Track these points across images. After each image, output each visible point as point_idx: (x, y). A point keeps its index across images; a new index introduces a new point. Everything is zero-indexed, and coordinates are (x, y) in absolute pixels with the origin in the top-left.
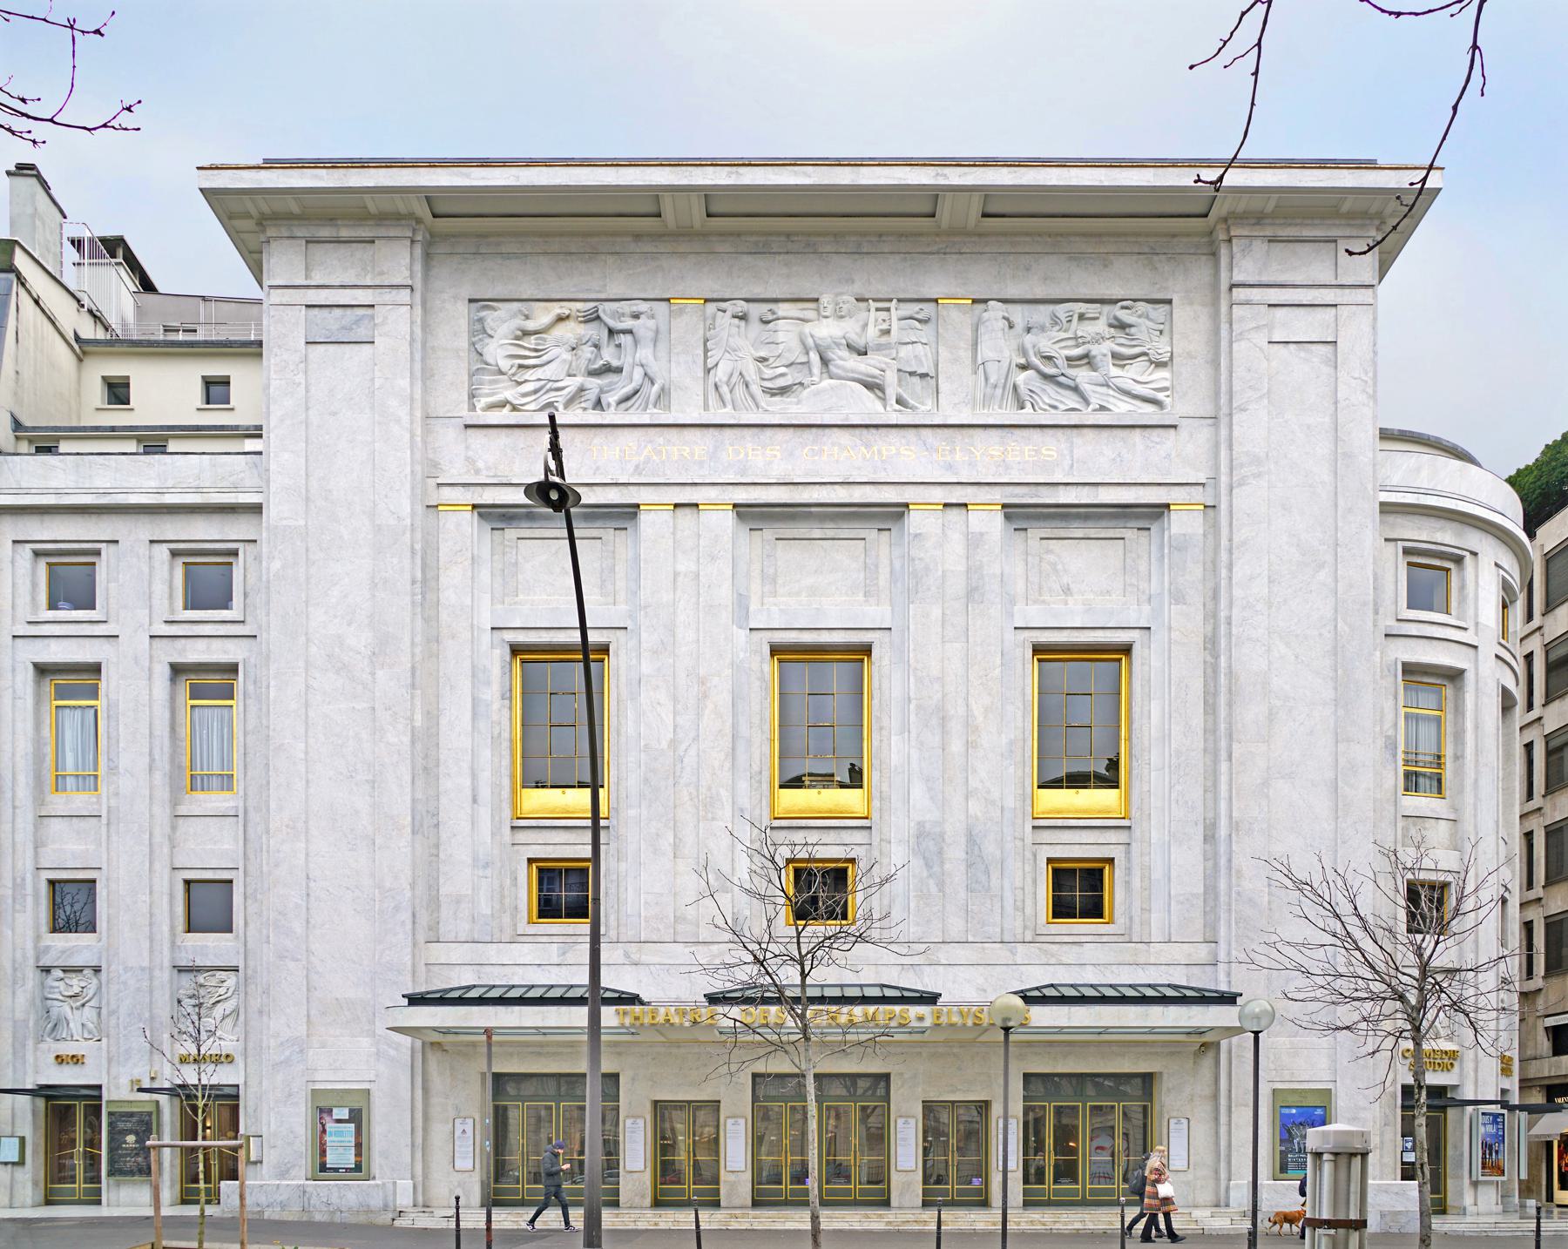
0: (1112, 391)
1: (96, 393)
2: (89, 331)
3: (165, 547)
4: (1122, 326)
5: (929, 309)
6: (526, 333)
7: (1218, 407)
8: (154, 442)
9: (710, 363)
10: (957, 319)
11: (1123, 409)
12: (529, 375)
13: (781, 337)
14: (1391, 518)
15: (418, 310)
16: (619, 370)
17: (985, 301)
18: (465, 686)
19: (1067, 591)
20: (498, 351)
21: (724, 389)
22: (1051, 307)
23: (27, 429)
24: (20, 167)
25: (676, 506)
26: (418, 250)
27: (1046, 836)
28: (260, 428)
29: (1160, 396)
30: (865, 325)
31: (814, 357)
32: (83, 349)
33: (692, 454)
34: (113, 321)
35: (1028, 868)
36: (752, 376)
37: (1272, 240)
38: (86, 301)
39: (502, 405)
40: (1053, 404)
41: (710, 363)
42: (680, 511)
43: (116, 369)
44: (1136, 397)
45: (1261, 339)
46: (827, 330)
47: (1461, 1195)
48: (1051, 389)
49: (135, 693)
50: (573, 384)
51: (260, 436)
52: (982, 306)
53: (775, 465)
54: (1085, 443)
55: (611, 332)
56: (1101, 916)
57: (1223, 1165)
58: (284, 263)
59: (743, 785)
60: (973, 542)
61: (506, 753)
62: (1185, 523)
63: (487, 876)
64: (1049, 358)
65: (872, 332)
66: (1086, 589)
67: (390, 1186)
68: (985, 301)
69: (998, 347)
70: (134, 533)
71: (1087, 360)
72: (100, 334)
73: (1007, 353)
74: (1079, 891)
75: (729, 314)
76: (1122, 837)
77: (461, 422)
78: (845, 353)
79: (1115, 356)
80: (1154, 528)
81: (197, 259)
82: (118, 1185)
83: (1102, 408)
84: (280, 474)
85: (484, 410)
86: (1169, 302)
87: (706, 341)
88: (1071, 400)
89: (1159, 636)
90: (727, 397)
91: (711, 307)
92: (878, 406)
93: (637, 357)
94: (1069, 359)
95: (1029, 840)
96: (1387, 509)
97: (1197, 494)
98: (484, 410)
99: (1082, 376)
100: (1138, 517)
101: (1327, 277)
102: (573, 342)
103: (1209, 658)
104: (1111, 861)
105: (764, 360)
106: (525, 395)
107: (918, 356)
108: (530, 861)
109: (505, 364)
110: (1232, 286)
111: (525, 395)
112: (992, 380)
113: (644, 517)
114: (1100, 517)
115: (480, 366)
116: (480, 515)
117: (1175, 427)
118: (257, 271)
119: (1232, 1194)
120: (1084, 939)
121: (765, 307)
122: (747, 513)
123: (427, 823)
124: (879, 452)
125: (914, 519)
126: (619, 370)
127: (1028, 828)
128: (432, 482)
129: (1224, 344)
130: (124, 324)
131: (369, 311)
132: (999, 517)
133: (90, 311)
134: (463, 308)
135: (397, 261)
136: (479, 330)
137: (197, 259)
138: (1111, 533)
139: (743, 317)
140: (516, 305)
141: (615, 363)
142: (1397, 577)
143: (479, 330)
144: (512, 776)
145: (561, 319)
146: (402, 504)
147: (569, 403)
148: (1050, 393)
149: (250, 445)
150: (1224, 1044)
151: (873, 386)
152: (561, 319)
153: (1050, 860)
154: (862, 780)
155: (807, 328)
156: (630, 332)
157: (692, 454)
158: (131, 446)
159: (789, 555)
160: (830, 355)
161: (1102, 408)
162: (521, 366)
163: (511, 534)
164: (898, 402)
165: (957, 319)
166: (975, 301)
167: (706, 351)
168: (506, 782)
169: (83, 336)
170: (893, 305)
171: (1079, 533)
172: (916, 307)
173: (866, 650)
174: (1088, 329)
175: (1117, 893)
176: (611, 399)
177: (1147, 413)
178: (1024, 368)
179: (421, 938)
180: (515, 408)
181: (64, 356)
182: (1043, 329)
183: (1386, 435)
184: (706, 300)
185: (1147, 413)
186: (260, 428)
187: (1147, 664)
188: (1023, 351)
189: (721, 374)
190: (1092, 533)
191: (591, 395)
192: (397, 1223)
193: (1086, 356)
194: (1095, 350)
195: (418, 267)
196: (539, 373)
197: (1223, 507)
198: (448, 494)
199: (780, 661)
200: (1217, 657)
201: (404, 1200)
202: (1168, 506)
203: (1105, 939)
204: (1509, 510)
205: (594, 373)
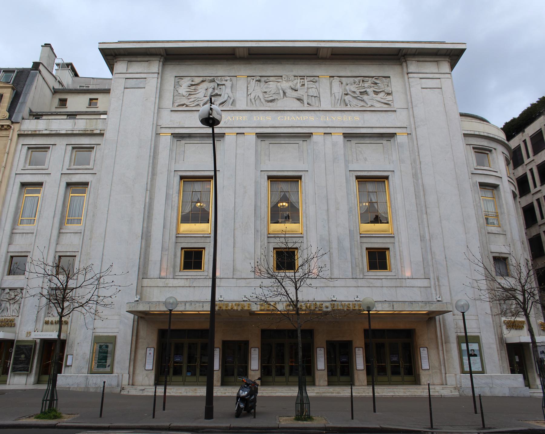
1: (56, 102)
2: (57, 86)
3: (71, 146)
4: (376, 84)
5: (317, 78)
7: (408, 106)
8: (72, 115)
9: (249, 93)
10: (324, 83)
11: (379, 106)
12: (192, 96)
13: (271, 86)
14: (467, 138)
15: (160, 79)
16: (220, 95)
17: (333, 77)
18: (164, 189)
19: (366, 159)
20: (183, 90)
21: (253, 100)
22: (353, 78)
23: (33, 112)
24: (46, 44)
25: (237, 134)
26: (161, 63)
27: (365, 240)
28: (107, 112)
29: (390, 102)
32: (55, 92)
33: (243, 118)
34: (65, 84)
35: (359, 251)
36: (261, 96)
37: (418, 61)
38: (58, 79)
39: (183, 105)
40: (355, 104)
41: (249, 93)
42: (238, 135)
43: (63, 96)
44: (382, 103)
45: (419, 87)
46: (285, 85)
47: (535, 380)
48: (355, 100)
49: (53, 192)
51: (106, 114)
52: (332, 78)
53: (268, 121)
54: (367, 115)
55: (218, 85)
56: (386, 269)
57: (442, 367)
58: (120, 66)
59: (258, 222)
60: (334, 145)
61: (176, 211)
62: (401, 138)
63: (164, 255)
64: (354, 92)
65: (299, 85)
67: (121, 376)
68: (333, 77)
69: (337, 89)
70: (61, 143)
71: (365, 93)
72: (61, 87)
73: (341, 90)
74: (378, 259)
75: (255, 80)
76: (391, 240)
77: (170, 110)
78: (291, 91)
79: (374, 91)
80: (392, 140)
81: (94, 68)
82: (15, 375)
83: (372, 106)
84: (110, 125)
85: (177, 106)
86: (389, 77)
87: (247, 87)
88: (362, 104)
89: (397, 173)
90: (254, 103)
91: (249, 78)
92: (302, 105)
93: (226, 92)
94: (360, 92)
95: (359, 242)
96: (465, 135)
97: (404, 130)
98: (177, 106)
99: (365, 97)
100: (386, 137)
101: (436, 71)
102: (206, 88)
103: (415, 181)
104: (388, 249)
105: (266, 92)
106: (191, 102)
107: (313, 92)
108: (182, 249)
109: (185, 94)
110: (408, 74)
111: (191, 102)
112: (337, 98)
113: (226, 137)
115: (176, 94)
116: (173, 136)
117: (395, 111)
118: (111, 69)
119: (448, 379)
120: (381, 277)
121: (266, 78)
122: (260, 136)
123: (146, 236)
124: (303, 118)
125: (314, 138)
126: (220, 95)
127: (359, 237)
128: (159, 127)
129: (408, 89)
130: (68, 85)
131: (145, 80)
132: (342, 137)
133: (59, 81)
134: (173, 79)
135: (155, 66)
136: (177, 85)
137: (94, 68)
138: (378, 142)
139: (259, 81)
140: (189, 78)
141: (219, 93)
142: (472, 156)
143: (177, 85)
144: (178, 219)
145: (203, 81)
146: (149, 133)
148: (355, 102)
149: (103, 117)
150: (437, 317)
152: (203, 81)
153: (367, 249)
154: (299, 220)
155: (279, 84)
156: (224, 85)
157: (243, 118)
158: (65, 117)
159: (274, 149)
160: (286, 91)
163: (183, 142)
164: (308, 104)
165: (324, 83)
166: (330, 77)
167: (247, 90)
168: (175, 221)
169: (55, 88)
170: (305, 78)
171: (368, 142)
172: (313, 78)
173: (300, 177)
174: (366, 85)
175: (392, 259)
177: (386, 108)
178: (347, 94)
179: (141, 277)
180: (187, 106)
181: (49, 93)
182: (351, 85)
183: (462, 115)
184: (248, 76)
185: (386, 108)
186: (107, 112)
187: (394, 181)
188: (346, 90)
189: (252, 96)
190: (372, 142)
192: (122, 393)
193: (366, 91)
194: (368, 90)
195: (161, 68)
196: (195, 96)
197: (414, 134)
198: (163, 130)
199: (271, 181)
200: (417, 180)
201: (125, 382)
202: (396, 134)
203: (389, 277)
204: (502, 136)
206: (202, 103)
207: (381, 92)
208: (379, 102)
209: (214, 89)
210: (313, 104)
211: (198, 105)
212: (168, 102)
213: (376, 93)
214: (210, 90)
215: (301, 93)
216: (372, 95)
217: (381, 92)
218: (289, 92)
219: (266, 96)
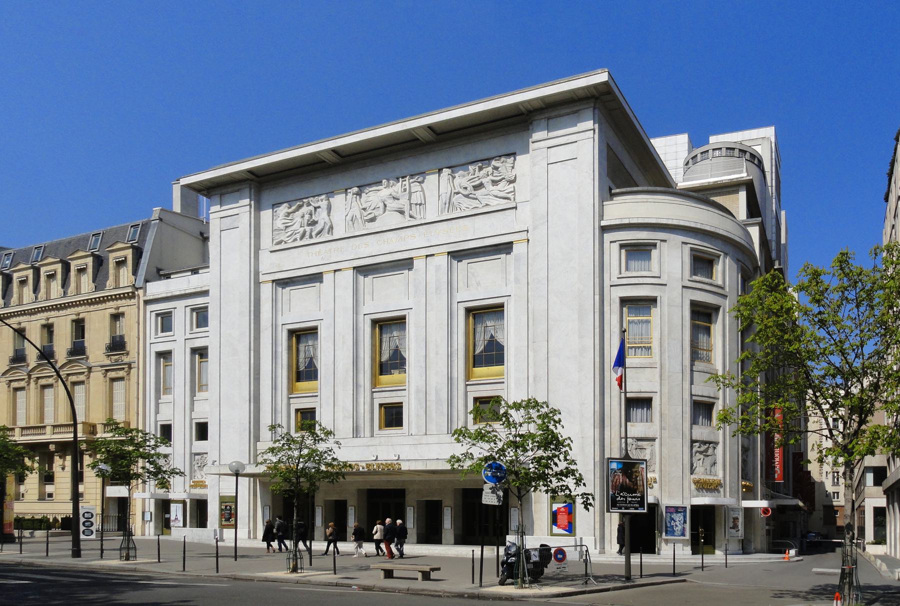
0: (489, 197)
6: (289, 214)
29: (510, 195)
30: (397, 188)
31: (381, 205)
40: (466, 206)
50: (302, 230)
64: (466, 188)
66: (483, 282)
71: (480, 186)
78: (391, 201)
83: (487, 205)
88: (475, 203)
94: (474, 187)
99: (478, 193)
105: (364, 209)
107: (416, 198)
114: (489, 251)
147: (301, 238)
151: (402, 212)
161: (487, 205)
162: (287, 227)
176: (314, 234)
177: (504, 204)
178: (458, 193)
191: (308, 234)
194: (484, 181)
205: (309, 225)
206: (298, 236)
207: (500, 180)
208: (496, 197)
209: (311, 214)
210: (418, 217)
211: (295, 240)
212: (266, 242)
213: (495, 183)
214: (307, 217)
215: (403, 203)
216: (490, 187)
217: (500, 180)
218: (392, 204)
219: (365, 213)
